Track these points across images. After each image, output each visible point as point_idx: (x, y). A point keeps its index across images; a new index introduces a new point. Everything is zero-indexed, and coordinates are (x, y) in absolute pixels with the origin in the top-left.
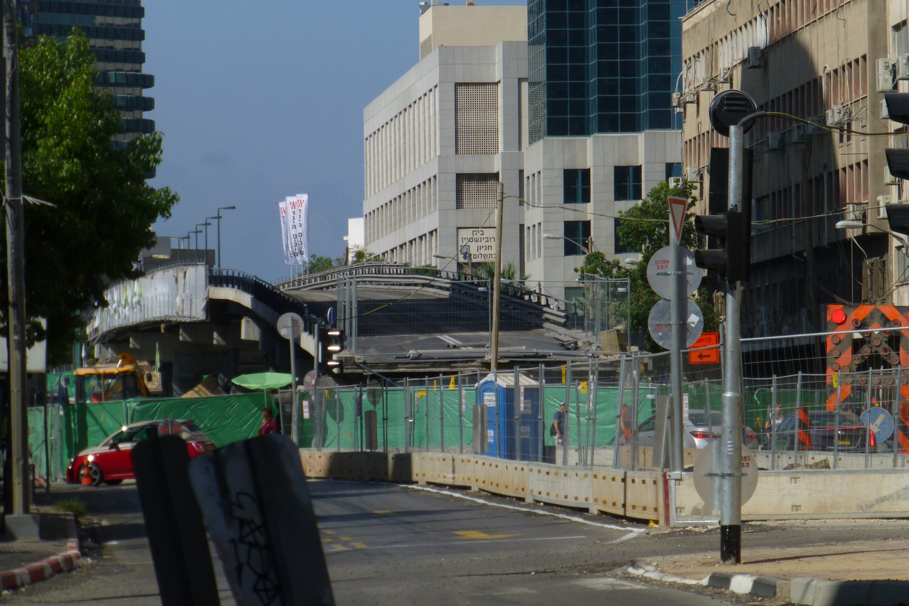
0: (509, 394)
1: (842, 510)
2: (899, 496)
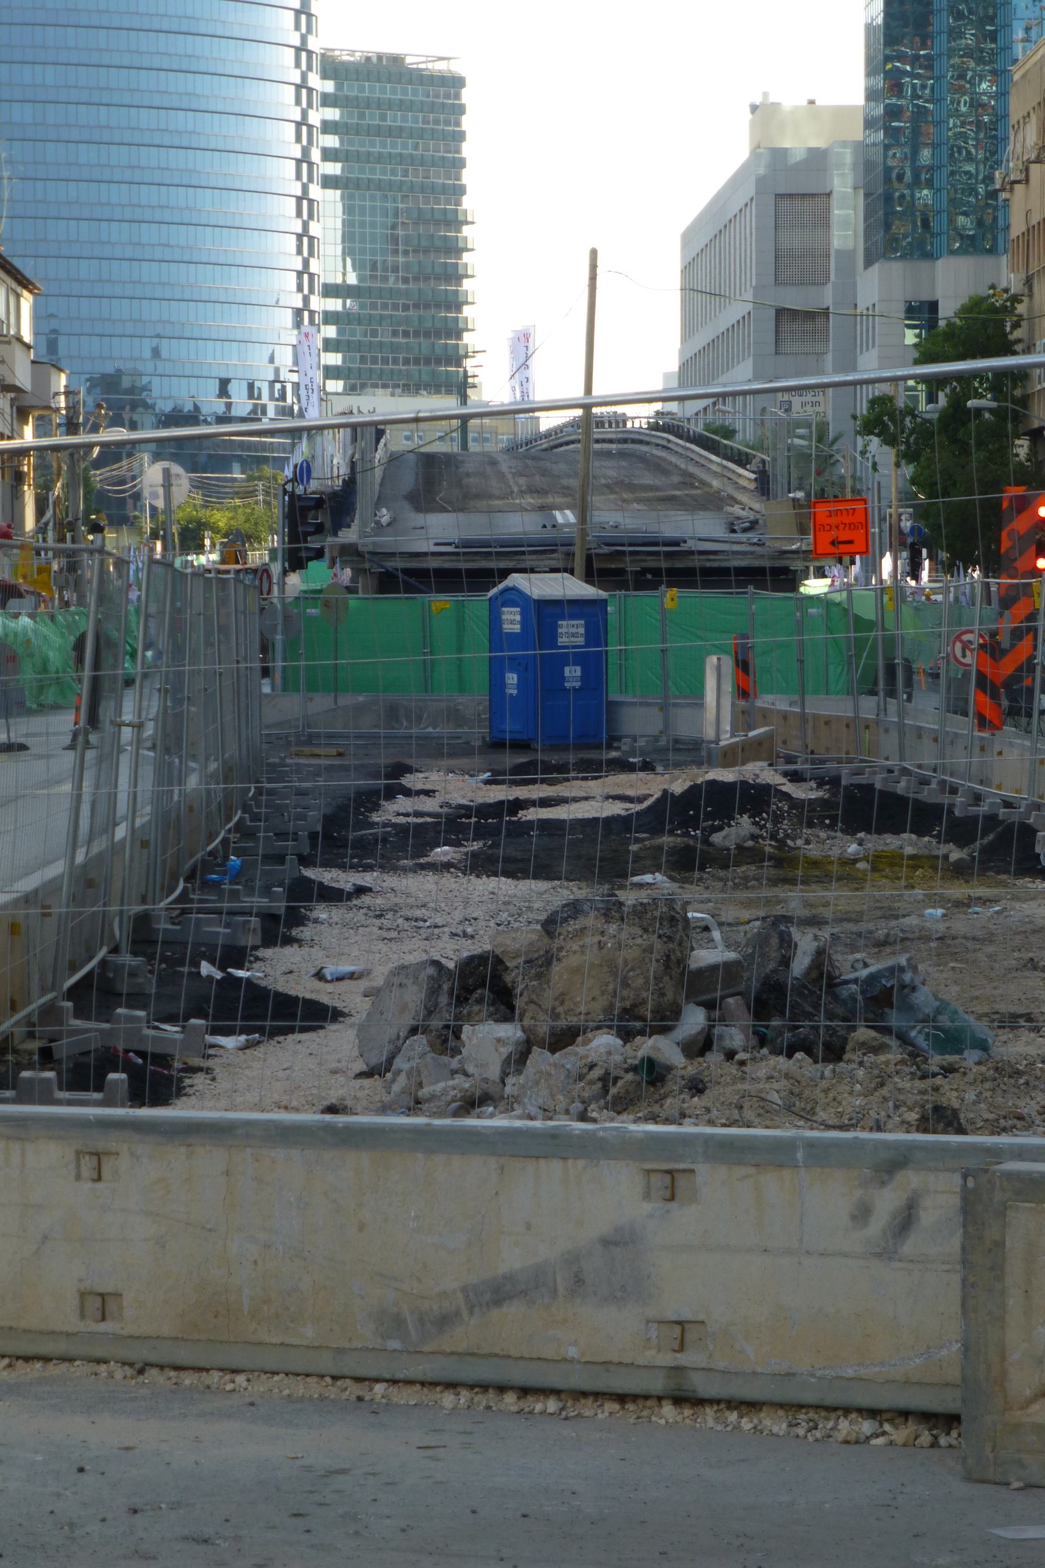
0: (546, 613)
1: (309, 1333)
2: (579, 1280)
